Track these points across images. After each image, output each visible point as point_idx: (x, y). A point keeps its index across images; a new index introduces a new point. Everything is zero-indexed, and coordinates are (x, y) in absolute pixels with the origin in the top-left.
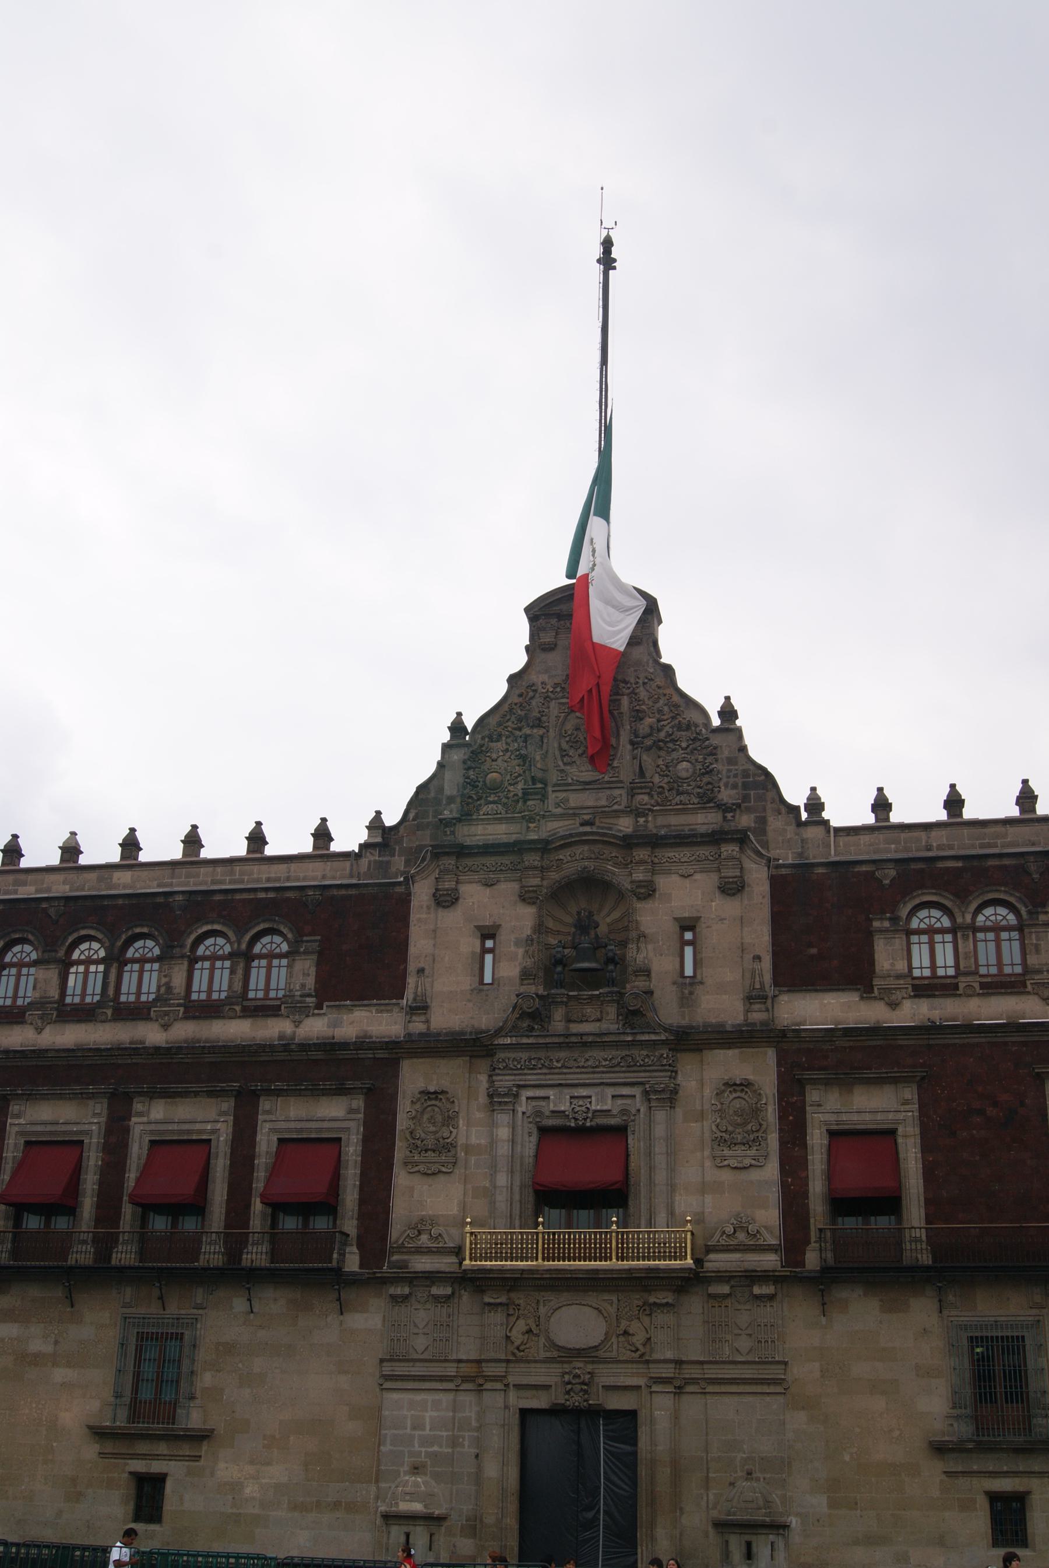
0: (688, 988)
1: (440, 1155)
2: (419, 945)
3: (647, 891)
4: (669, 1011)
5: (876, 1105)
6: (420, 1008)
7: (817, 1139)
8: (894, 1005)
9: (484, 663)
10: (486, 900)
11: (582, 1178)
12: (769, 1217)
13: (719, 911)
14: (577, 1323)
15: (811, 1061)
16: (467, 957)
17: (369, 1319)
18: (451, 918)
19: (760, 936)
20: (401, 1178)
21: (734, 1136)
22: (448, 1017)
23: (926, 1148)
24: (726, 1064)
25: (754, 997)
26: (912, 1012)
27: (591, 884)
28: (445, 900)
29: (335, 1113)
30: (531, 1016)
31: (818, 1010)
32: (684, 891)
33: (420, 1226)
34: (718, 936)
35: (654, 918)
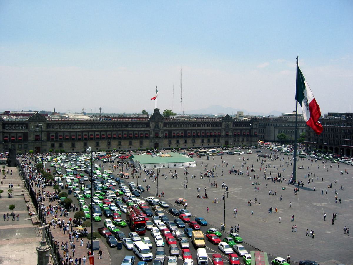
0: (161, 127)
1: (151, 134)
2: (150, 125)
3: (159, 123)
5: (167, 132)
6: (150, 128)
10: (153, 123)
11: (156, 134)
12: (163, 136)
14: (157, 140)
15: (165, 130)
16: (152, 125)
17: (149, 140)
18: (152, 124)
19: (163, 125)
21: (162, 133)
22: (151, 128)
24: (162, 130)
25: (163, 128)
26: (168, 129)
27: (157, 123)
28: (151, 123)
29: (147, 132)
31: (165, 128)
32: (160, 123)
33: (151, 137)
34: (162, 125)
35: (159, 124)
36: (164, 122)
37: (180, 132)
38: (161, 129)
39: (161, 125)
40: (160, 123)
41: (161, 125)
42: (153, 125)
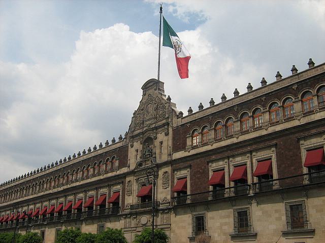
2: (129, 154)
4: (158, 161)
5: (185, 173)
6: (129, 167)
7: (176, 181)
8: (189, 152)
9: (134, 100)
12: (169, 197)
13: (166, 138)
15: (175, 164)
19: (170, 143)
20: (126, 197)
23: (191, 179)
25: (170, 155)
28: (132, 146)
29: (119, 187)
30: (140, 164)
32: (161, 137)
34: (165, 144)
35: (157, 143)
36: (175, 125)
37: (251, 162)
38: (159, 166)
39: (164, 140)
40: (161, 137)
41: (161, 143)
42: (137, 151)
